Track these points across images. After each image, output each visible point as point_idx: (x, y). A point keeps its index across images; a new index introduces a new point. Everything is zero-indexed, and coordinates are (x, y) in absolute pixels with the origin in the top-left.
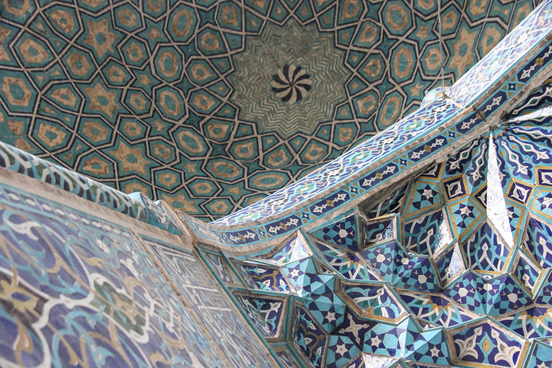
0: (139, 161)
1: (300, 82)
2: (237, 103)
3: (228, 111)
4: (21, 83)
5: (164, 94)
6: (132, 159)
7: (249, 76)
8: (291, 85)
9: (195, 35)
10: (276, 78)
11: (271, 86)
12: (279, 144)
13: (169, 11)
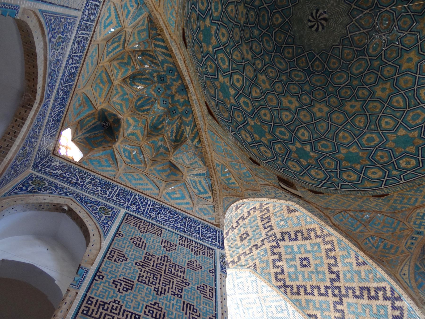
0: (407, 57)
1: (315, 17)
2: (339, 41)
3: (346, 42)
4: (409, 118)
5: (355, 72)
6: (410, 60)
7: (321, 43)
8: (317, 21)
9: (319, 73)
10: (317, 30)
11: (322, 30)
12: (355, 7)
13: (318, 88)
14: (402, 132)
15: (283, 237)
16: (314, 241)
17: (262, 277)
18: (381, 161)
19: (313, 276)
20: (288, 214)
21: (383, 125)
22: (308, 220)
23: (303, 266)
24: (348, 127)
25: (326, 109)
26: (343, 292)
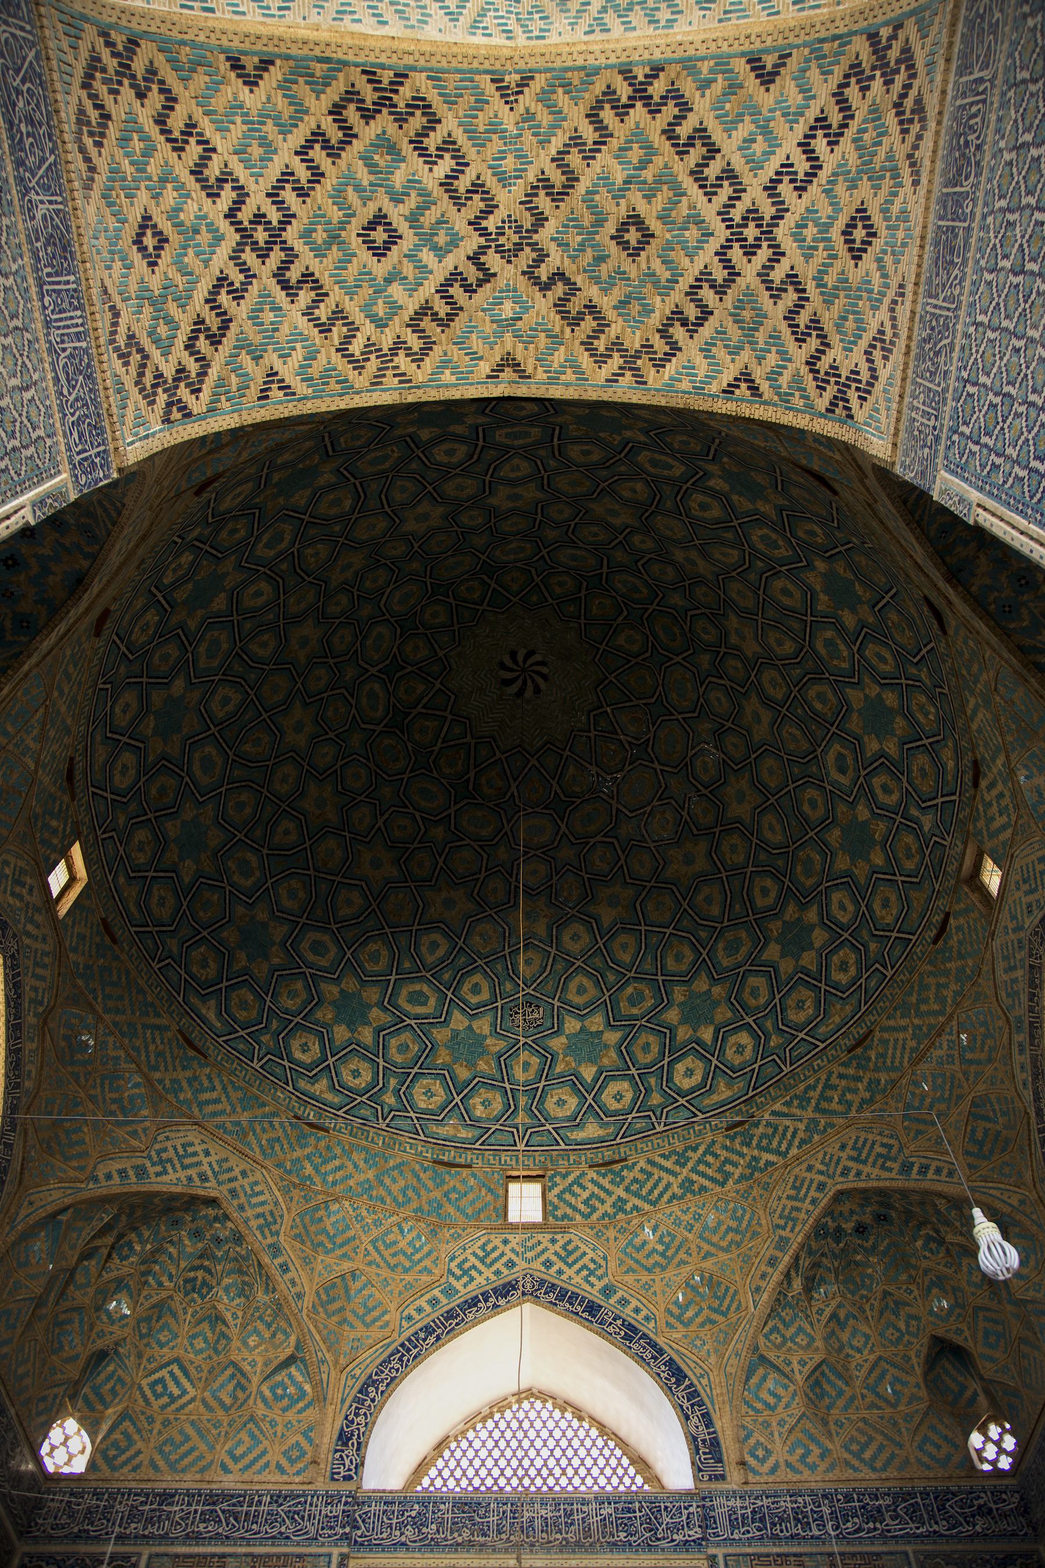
10: (513, 655)
14: (220, 603)
15: (481, 267)
16: (396, 327)
17: (465, 66)
18: (230, 525)
19: (336, 214)
20: (509, 347)
21: (264, 586)
22: (447, 372)
23: (379, 220)
24: (337, 528)
25: (411, 526)
26: (249, 257)
